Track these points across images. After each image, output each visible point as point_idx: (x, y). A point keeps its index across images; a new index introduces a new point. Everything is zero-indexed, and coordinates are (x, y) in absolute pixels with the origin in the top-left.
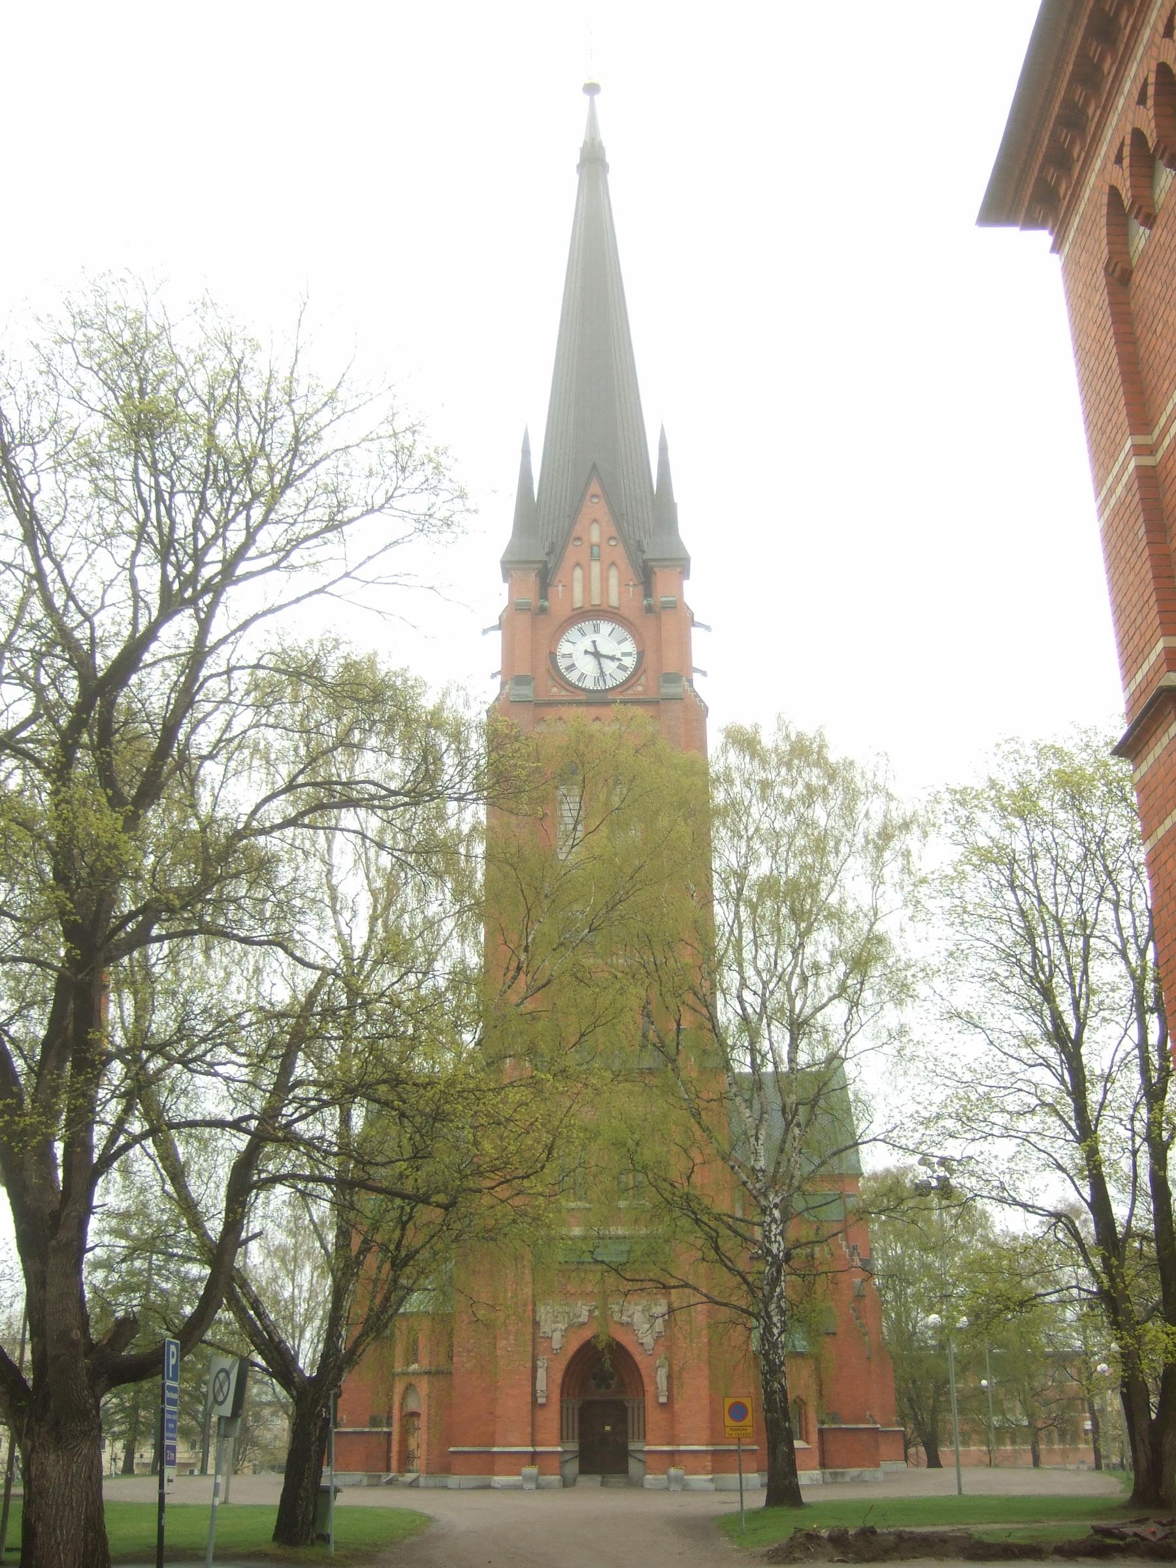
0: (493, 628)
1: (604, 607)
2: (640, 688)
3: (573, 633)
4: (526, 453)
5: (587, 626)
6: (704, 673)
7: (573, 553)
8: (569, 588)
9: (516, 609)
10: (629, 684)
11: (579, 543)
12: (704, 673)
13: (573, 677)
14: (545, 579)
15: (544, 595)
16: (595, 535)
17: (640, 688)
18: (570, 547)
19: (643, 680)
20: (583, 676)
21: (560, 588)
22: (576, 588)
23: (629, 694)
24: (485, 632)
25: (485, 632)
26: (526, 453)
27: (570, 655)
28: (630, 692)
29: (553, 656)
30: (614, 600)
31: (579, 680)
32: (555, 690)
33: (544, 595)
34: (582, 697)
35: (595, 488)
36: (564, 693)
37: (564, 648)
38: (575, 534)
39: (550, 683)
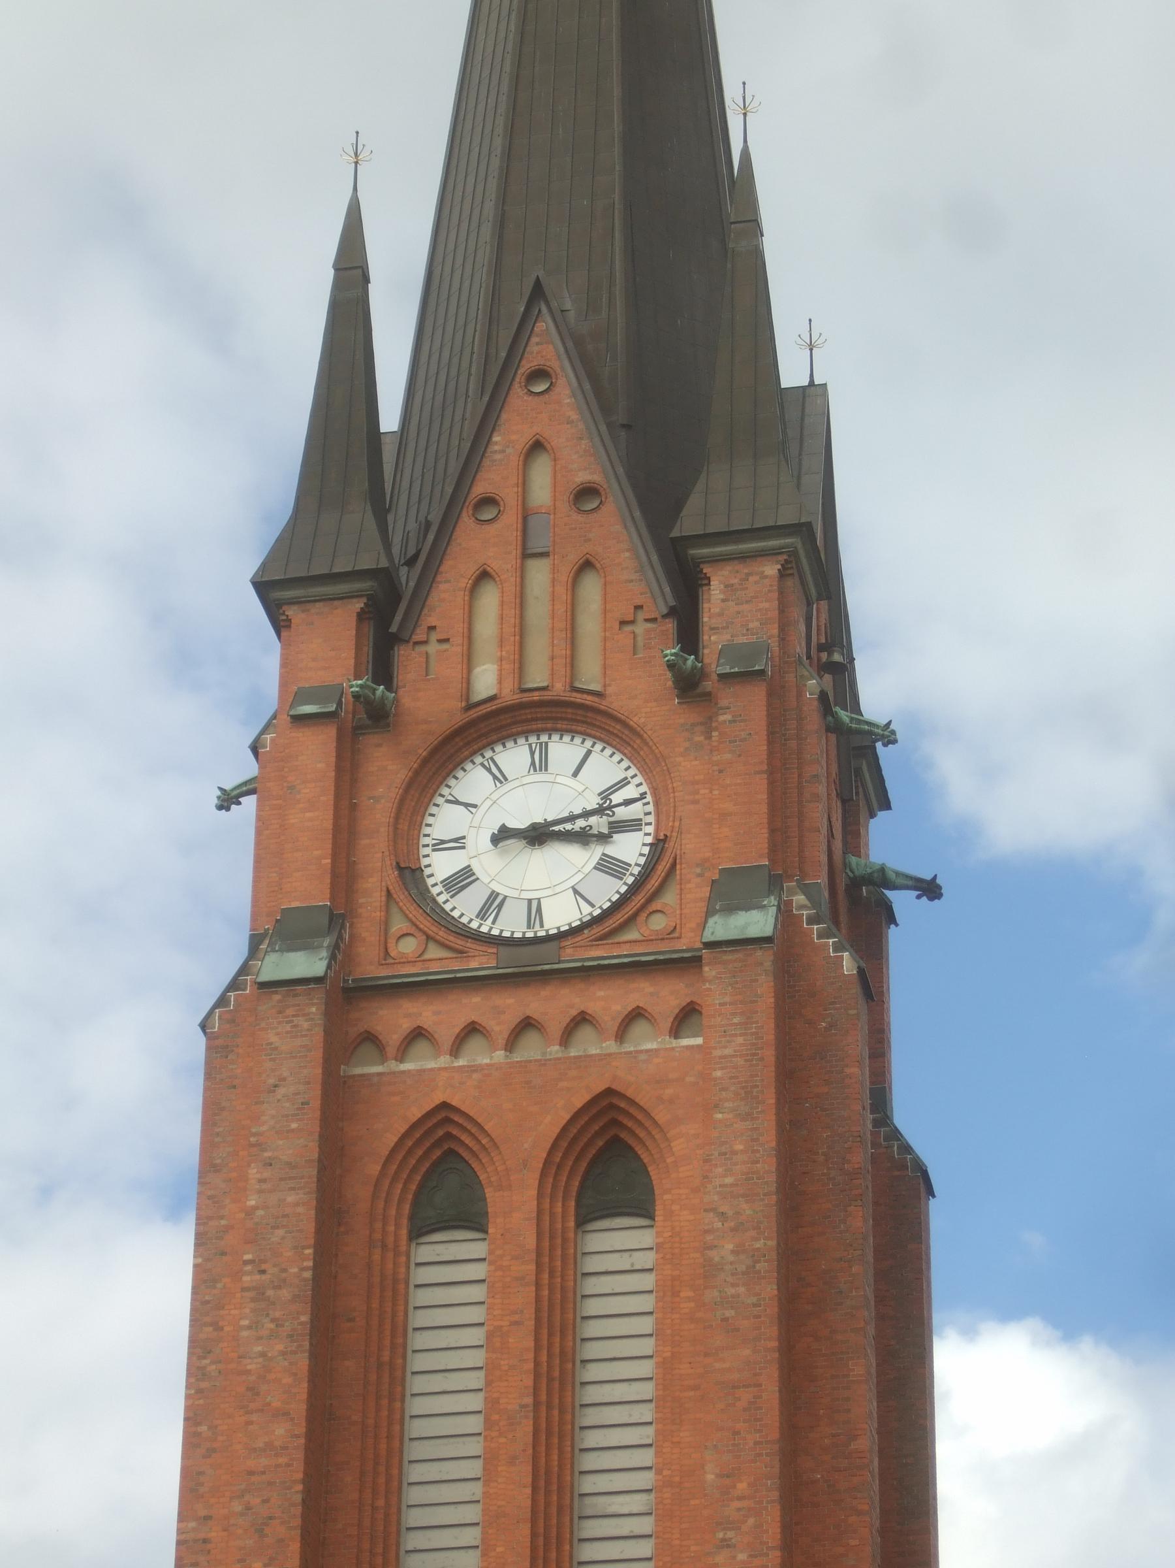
2: (658, 923)
6: (930, 889)
7: (478, 543)
9: (297, 711)
10: (628, 910)
11: (487, 514)
12: (930, 889)
14: (388, 616)
15: (382, 669)
16: (542, 485)
17: (658, 923)
18: (466, 520)
19: (669, 898)
22: (476, 645)
23: (632, 943)
24: (228, 800)
25: (228, 800)
27: (459, 843)
28: (632, 935)
30: (590, 675)
31: (482, 914)
33: (382, 669)
34: (481, 962)
35: (545, 347)
36: (434, 952)
38: (480, 489)
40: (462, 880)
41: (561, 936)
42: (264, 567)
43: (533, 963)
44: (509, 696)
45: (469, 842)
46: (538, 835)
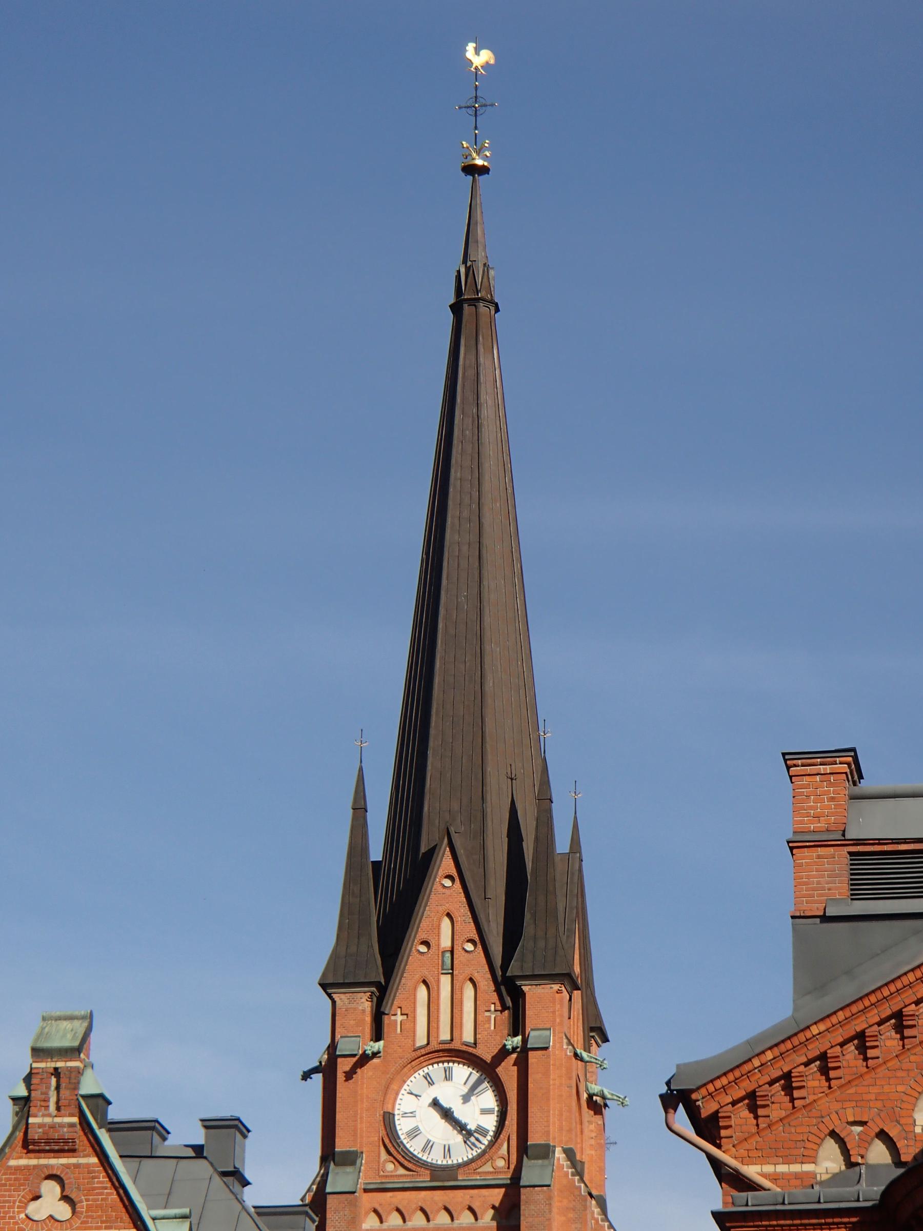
0: (315, 1070)
1: (456, 1045)
3: (416, 1081)
4: (360, 809)
5: (435, 1071)
8: (410, 1015)
11: (423, 949)
13: (415, 1147)
20: (428, 1146)
21: (399, 1018)
24: (306, 1076)
25: (306, 1076)
26: (360, 809)
27: (412, 1114)
29: (388, 1120)
31: (424, 1150)
32: (390, 1167)
34: (424, 1178)
36: (402, 1171)
37: (404, 1103)
39: (384, 1155)
40: (414, 1133)
41: (459, 1166)
42: (324, 975)
43: (444, 1178)
44: (434, 1045)
45: (417, 1114)
46: (447, 1114)
